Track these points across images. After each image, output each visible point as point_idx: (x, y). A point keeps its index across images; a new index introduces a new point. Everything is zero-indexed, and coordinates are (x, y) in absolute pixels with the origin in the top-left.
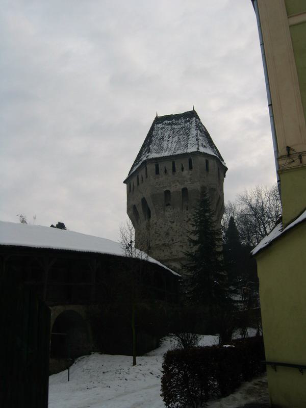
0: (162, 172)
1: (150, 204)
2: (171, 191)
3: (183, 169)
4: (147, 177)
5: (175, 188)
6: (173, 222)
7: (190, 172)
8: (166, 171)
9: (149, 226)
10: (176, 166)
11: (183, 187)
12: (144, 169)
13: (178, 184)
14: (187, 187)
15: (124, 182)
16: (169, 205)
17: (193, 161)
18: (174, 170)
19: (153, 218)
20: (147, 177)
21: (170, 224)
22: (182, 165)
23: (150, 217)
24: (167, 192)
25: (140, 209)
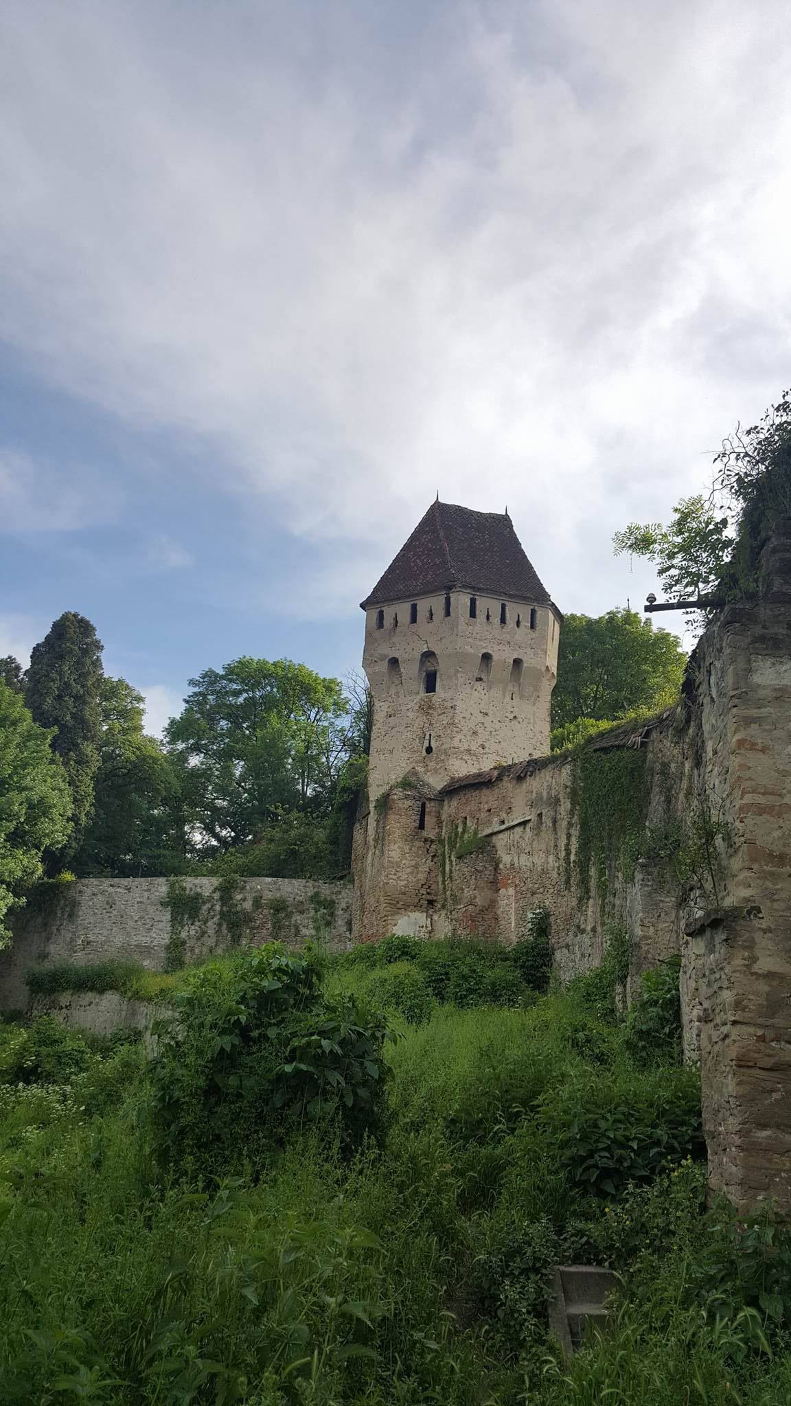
0: (481, 616)
1: (443, 667)
2: (495, 657)
4: (448, 614)
5: (503, 656)
8: (488, 617)
10: (508, 615)
12: (442, 600)
16: (480, 679)
18: (503, 620)
20: (448, 614)
23: (430, 687)
24: (486, 657)
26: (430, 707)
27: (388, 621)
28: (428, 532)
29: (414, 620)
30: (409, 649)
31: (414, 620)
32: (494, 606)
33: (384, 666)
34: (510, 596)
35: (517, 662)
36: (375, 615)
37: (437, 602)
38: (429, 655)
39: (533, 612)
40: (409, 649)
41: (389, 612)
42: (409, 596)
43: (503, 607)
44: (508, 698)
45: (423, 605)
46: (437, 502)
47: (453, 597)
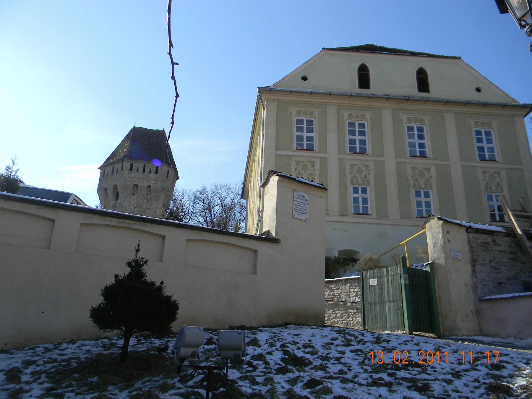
3: (150, 172)
4: (122, 170)
5: (143, 184)
7: (156, 176)
8: (137, 170)
9: (116, 206)
11: (148, 184)
15: (99, 168)
16: (134, 194)
18: (144, 171)
20: (122, 170)
23: (117, 199)
25: (110, 192)
26: (116, 206)
31: (112, 173)
47: (124, 163)
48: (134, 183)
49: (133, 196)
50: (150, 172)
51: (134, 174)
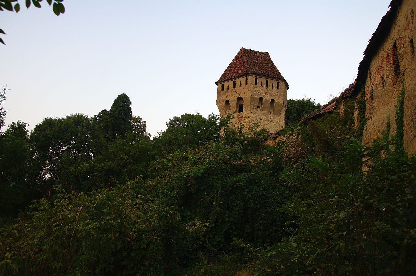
1: (246, 102)
2: (264, 99)
3: (273, 87)
4: (247, 83)
5: (267, 98)
6: (262, 120)
7: (278, 91)
8: (261, 84)
10: (269, 84)
13: (269, 95)
14: (275, 100)
16: (259, 107)
17: (280, 84)
18: (267, 86)
19: (245, 112)
20: (247, 83)
21: (259, 120)
22: (273, 84)
24: (261, 99)
27: (225, 88)
28: (239, 58)
29: (234, 86)
30: (233, 97)
31: (234, 86)
32: (264, 81)
33: (223, 104)
34: (270, 77)
35: (273, 101)
36: (220, 85)
37: (243, 80)
38: (240, 99)
39: (278, 83)
40: (233, 97)
41: (226, 85)
42: (232, 79)
43: (267, 81)
44: (269, 114)
45: (238, 81)
46: (243, 48)
48: (261, 96)
49: (259, 109)
50: (273, 87)
51: (259, 87)
